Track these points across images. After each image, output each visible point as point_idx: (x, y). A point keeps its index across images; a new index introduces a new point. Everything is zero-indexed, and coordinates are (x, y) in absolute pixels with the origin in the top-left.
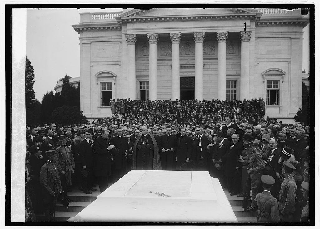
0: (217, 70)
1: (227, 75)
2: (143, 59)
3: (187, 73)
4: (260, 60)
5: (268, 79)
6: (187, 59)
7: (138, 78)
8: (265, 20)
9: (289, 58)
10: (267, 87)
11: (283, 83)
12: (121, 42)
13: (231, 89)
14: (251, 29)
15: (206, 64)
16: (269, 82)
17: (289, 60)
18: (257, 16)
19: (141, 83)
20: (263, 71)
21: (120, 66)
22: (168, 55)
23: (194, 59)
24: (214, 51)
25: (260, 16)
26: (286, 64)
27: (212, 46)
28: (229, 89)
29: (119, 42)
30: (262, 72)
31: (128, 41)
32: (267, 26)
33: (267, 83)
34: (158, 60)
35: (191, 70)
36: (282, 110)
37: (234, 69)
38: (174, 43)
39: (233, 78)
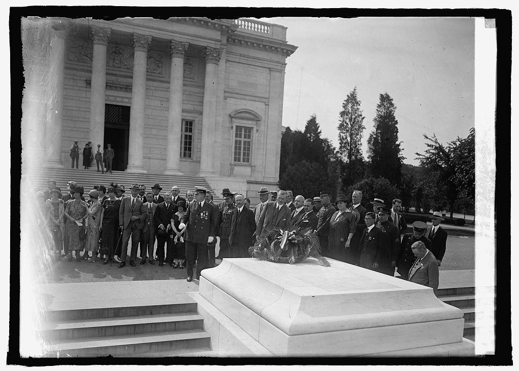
1: (183, 111)
3: (119, 98)
4: (227, 95)
5: (238, 124)
6: (116, 75)
8: (239, 36)
9: (267, 96)
10: (236, 136)
14: (222, 46)
16: (239, 128)
18: (232, 28)
23: (132, 77)
25: (235, 29)
26: (262, 106)
30: (229, 113)
33: (236, 131)
36: (254, 171)
37: (190, 103)
39: (189, 117)
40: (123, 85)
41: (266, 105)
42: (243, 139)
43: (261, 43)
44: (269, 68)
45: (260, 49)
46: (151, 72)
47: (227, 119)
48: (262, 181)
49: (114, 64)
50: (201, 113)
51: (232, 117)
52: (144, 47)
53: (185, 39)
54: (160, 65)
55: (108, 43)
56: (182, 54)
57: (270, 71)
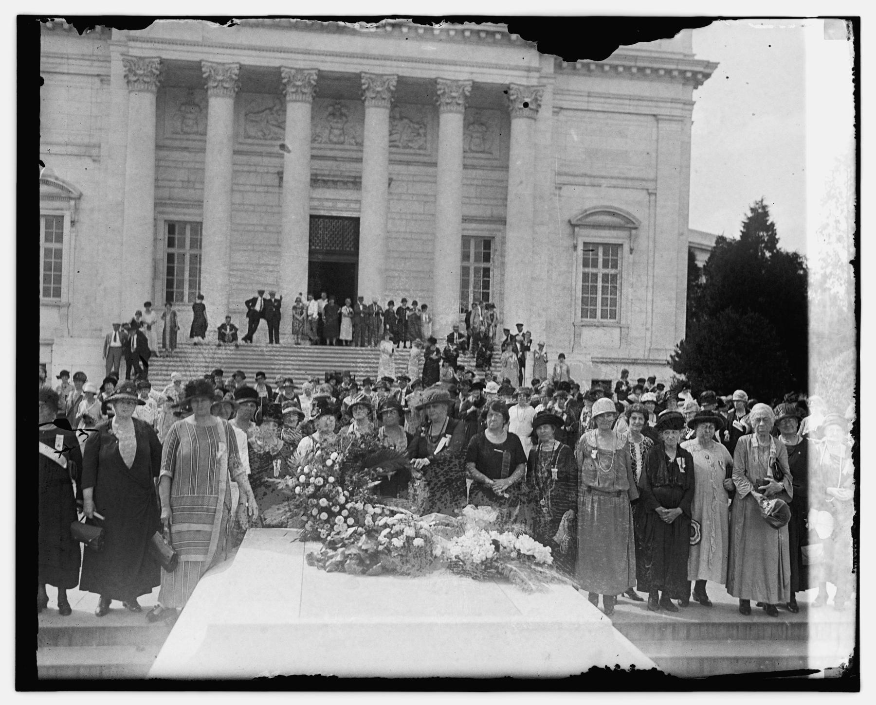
0: (431, 199)
1: (466, 219)
2: (185, 144)
5: (588, 240)
7: (161, 209)
9: (652, 176)
10: (585, 264)
11: (631, 253)
12: (104, 79)
13: (472, 264)
14: (544, 81)
15: (394, 177)
16: (590, 248)
17: (650, 185)
19: (172, 227)
20: (573, 211)
21: (94, 161)
22: (271, 139)
23: (359, 160)
24: (425, 139)
27: (418, 123)
28: (466, 264)
29: (97, 80)
30: (567, 217)
31: (132, 77)
32: (590, 76)
34: (236, 152)
35: (350, 194)
38: (295, 101)
40: (349, 177)
41: (649, 194)
42: (601, 271)
43: (632, 64)
44: (654, 115)
45: (632, 76)
46: (404, 147)
47: (568, 230)
48: (646, 357)
49: (332, 137)
50: (503, 221)
51: (573, 226)
52: (384, 99)
53: (463, 75)
54: (421, 131)
55: (314, 98)
56: (459, 104)
57: (657, 120)
